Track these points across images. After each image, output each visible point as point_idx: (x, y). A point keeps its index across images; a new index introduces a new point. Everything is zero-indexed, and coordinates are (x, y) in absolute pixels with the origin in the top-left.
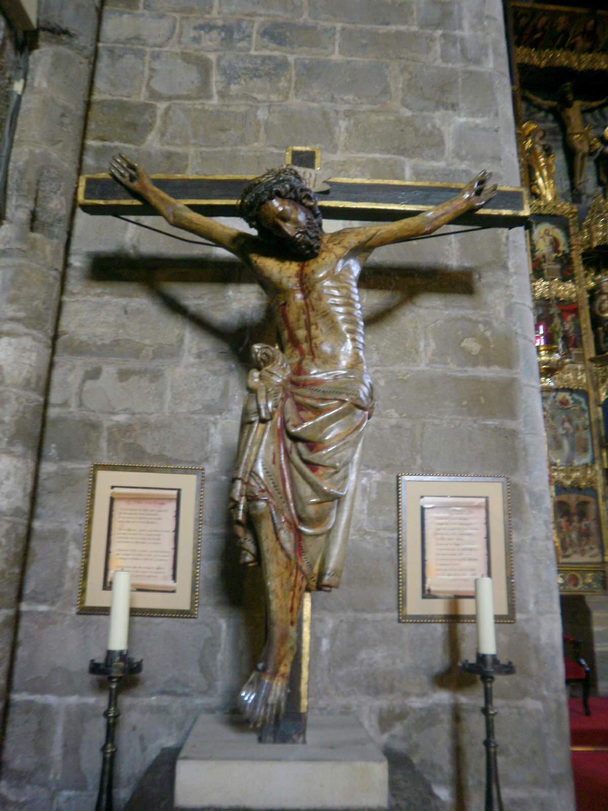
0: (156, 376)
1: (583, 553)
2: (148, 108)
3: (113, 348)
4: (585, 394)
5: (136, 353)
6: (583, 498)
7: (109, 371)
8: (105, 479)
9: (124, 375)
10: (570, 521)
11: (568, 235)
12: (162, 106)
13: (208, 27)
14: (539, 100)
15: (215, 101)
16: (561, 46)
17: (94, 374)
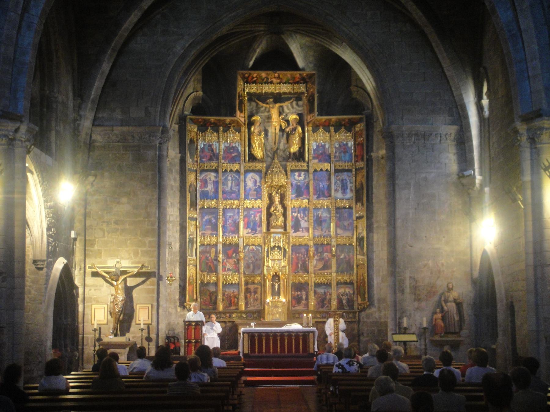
0: (100, 290)
1: (254, 306)
2: (95, 240)
3: (93, 286)
4: (261, 246)
5: (97, 286)
6: (256, 286)
7: (93, 289)
8: (93, 306)
9: (95, 290)
10: (251, 295)
11: (261, 178)
12: (97, 240)
13: (104, 222)
14: (260, 103)
15: (106, 238)
16: (267, 83)
17: (90, 290)
